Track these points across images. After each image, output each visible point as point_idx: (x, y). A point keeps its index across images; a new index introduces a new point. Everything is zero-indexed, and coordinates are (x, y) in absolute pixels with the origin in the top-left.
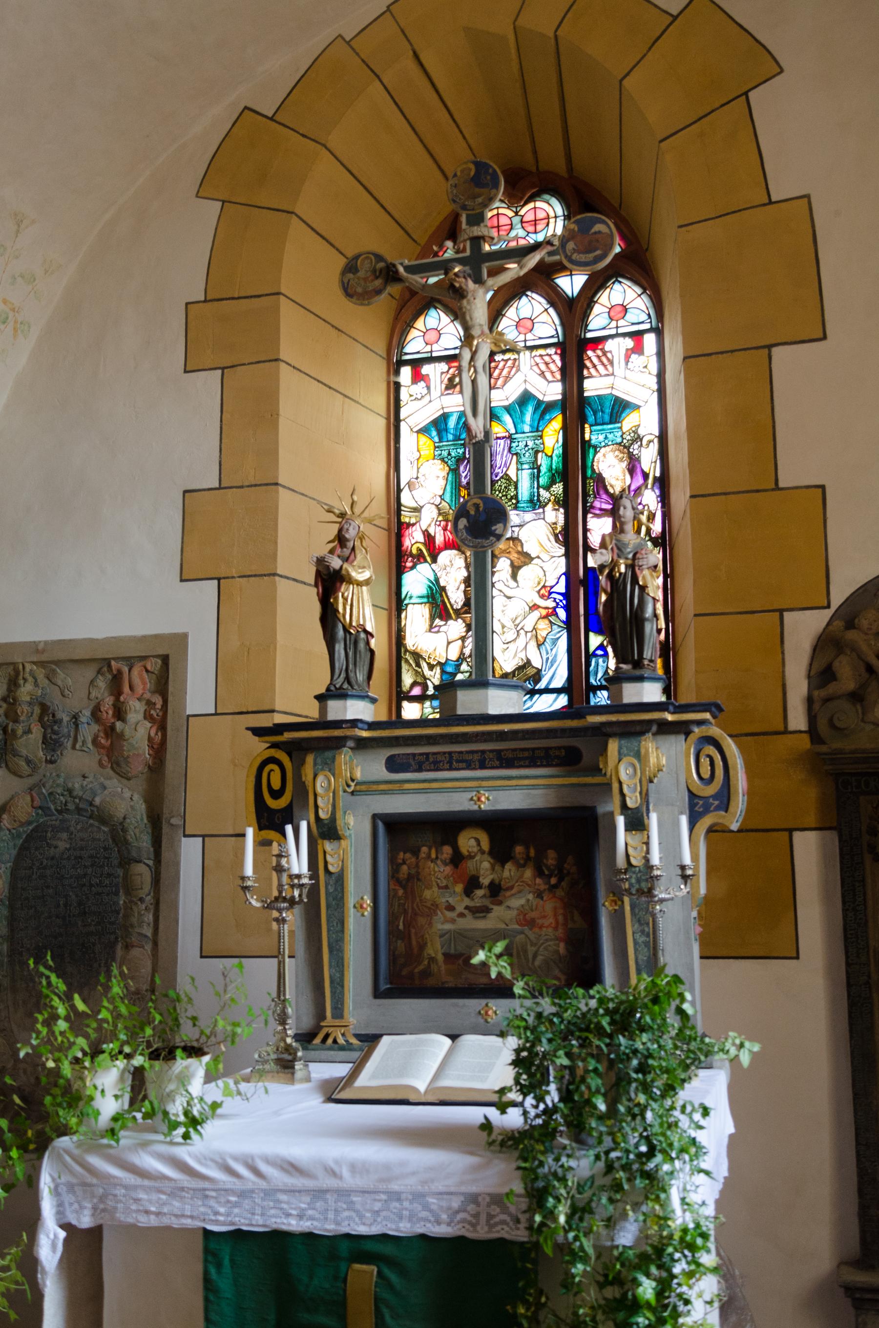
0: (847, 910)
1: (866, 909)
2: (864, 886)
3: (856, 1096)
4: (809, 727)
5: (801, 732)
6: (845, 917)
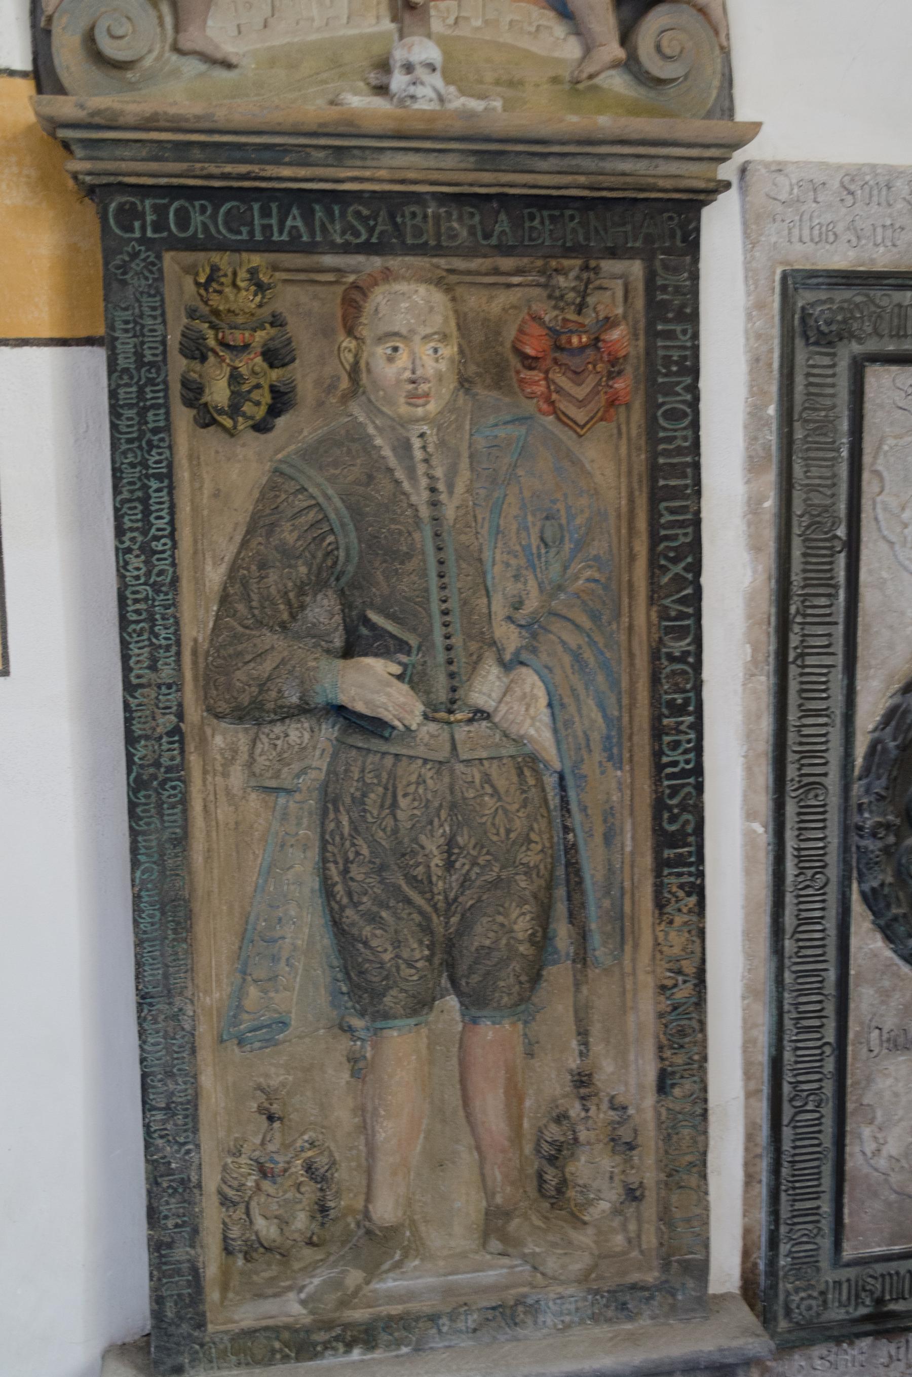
0: (129, 550)
1: (175, 546)
2: (171, 489)
3: (144, 1000)
4: (35, 61)
5: (11, 73)
6: (122, 568)
